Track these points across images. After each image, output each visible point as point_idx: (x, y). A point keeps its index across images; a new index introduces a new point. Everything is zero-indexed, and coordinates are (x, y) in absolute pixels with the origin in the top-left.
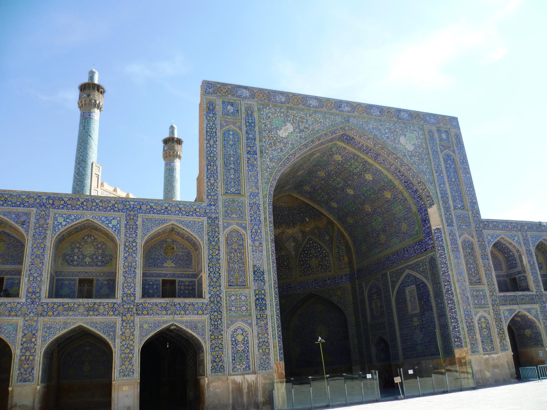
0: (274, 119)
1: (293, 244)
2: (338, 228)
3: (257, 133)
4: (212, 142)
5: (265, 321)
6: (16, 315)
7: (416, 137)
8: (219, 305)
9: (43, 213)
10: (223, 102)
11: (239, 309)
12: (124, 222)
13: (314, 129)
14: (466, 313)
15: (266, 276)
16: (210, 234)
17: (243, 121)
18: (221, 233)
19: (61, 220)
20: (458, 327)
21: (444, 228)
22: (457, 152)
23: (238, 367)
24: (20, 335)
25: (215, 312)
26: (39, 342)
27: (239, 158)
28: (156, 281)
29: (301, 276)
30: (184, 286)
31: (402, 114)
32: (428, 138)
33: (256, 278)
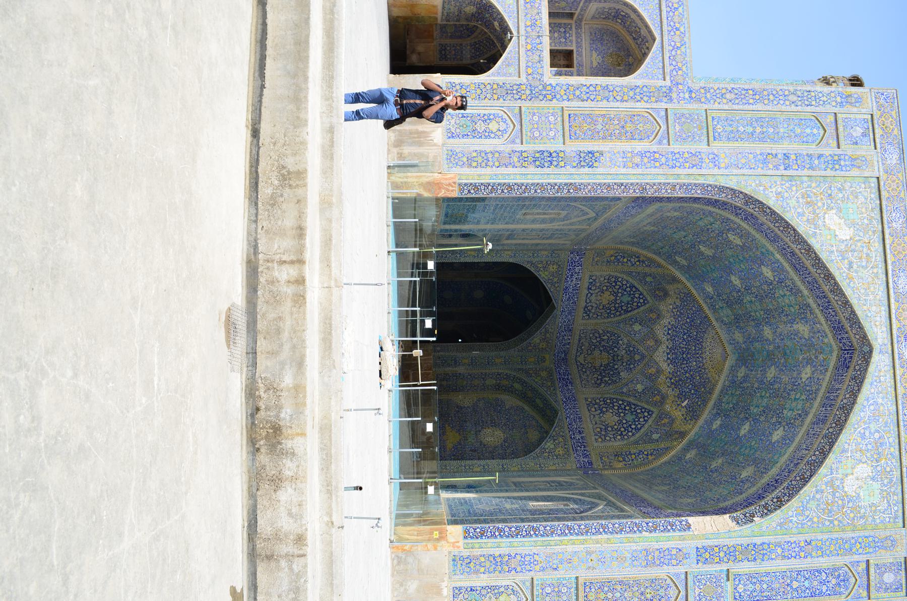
0: (855, 206)
1: (640, 387)
2: (675, 446)
3: (823, 173)
5: (518, 164)
8: (541, 97)
11: (536, 126)
13: (851, 279)
14: (528, 558)
15: (586, 170)
16: (645, 89)
18: (648, 106)
20: (501, 537)
21: (694, 537)
25: (531, 90)
27: (773, 141)
28: (571, 41)
29: (586, 399)
33: (582, 155)
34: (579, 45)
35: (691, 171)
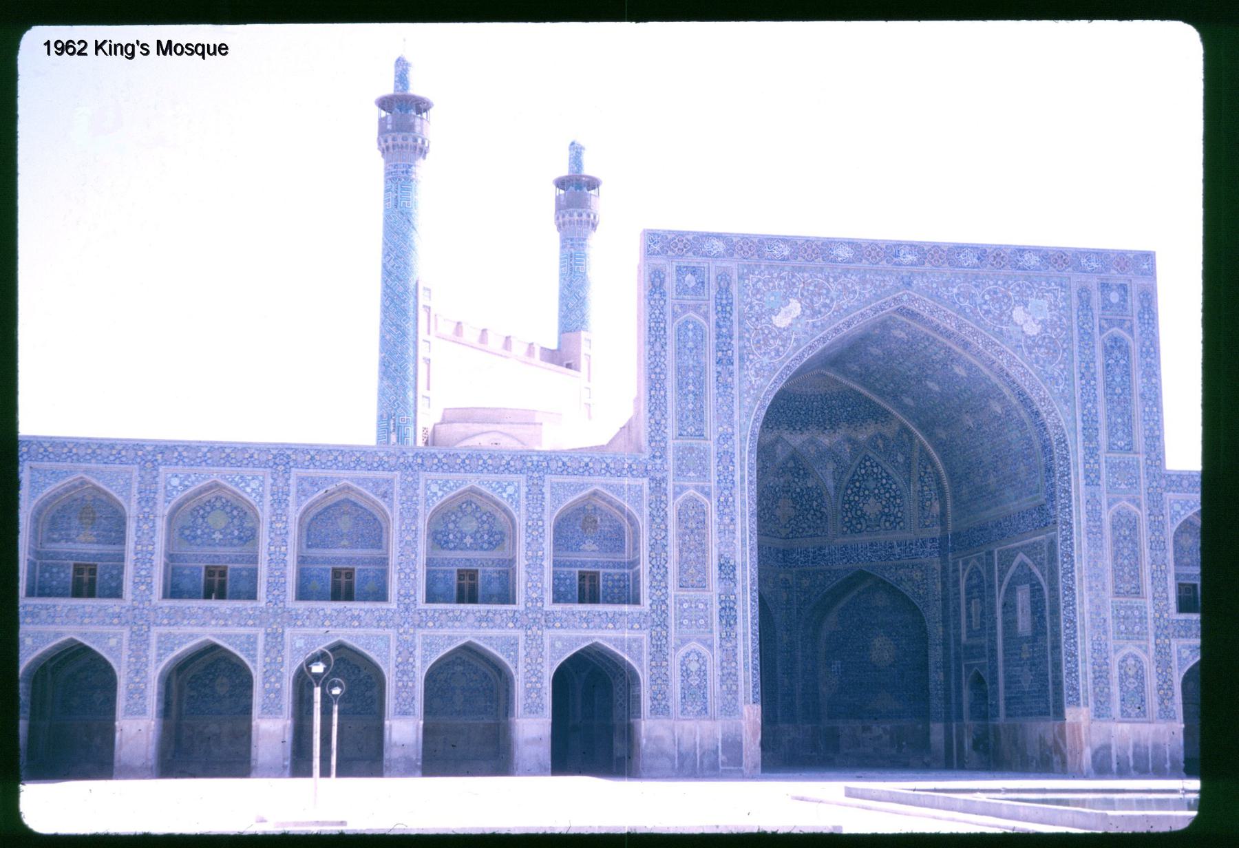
4: (658, 347)
6: (387, 627)
7: (1050, 304)
9: (410, 479)
10: (679, 269)
12: (524, 490)
13: (840, 307)
15: (738, 572)
17: (712, 303)
19: (435, 488)
22: (1137, 331)
23: (689, 708)
24: (393, 653)
26: (418, 663)
28: (570, 573)
30: (613, 581)
31: (1027, 256)
32: (1075, 307)
34: (576, 566)
35: (738, 467)
